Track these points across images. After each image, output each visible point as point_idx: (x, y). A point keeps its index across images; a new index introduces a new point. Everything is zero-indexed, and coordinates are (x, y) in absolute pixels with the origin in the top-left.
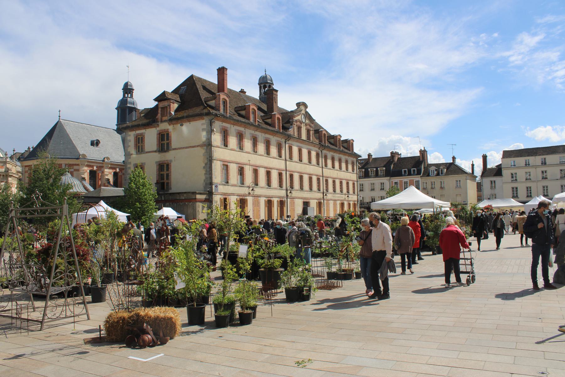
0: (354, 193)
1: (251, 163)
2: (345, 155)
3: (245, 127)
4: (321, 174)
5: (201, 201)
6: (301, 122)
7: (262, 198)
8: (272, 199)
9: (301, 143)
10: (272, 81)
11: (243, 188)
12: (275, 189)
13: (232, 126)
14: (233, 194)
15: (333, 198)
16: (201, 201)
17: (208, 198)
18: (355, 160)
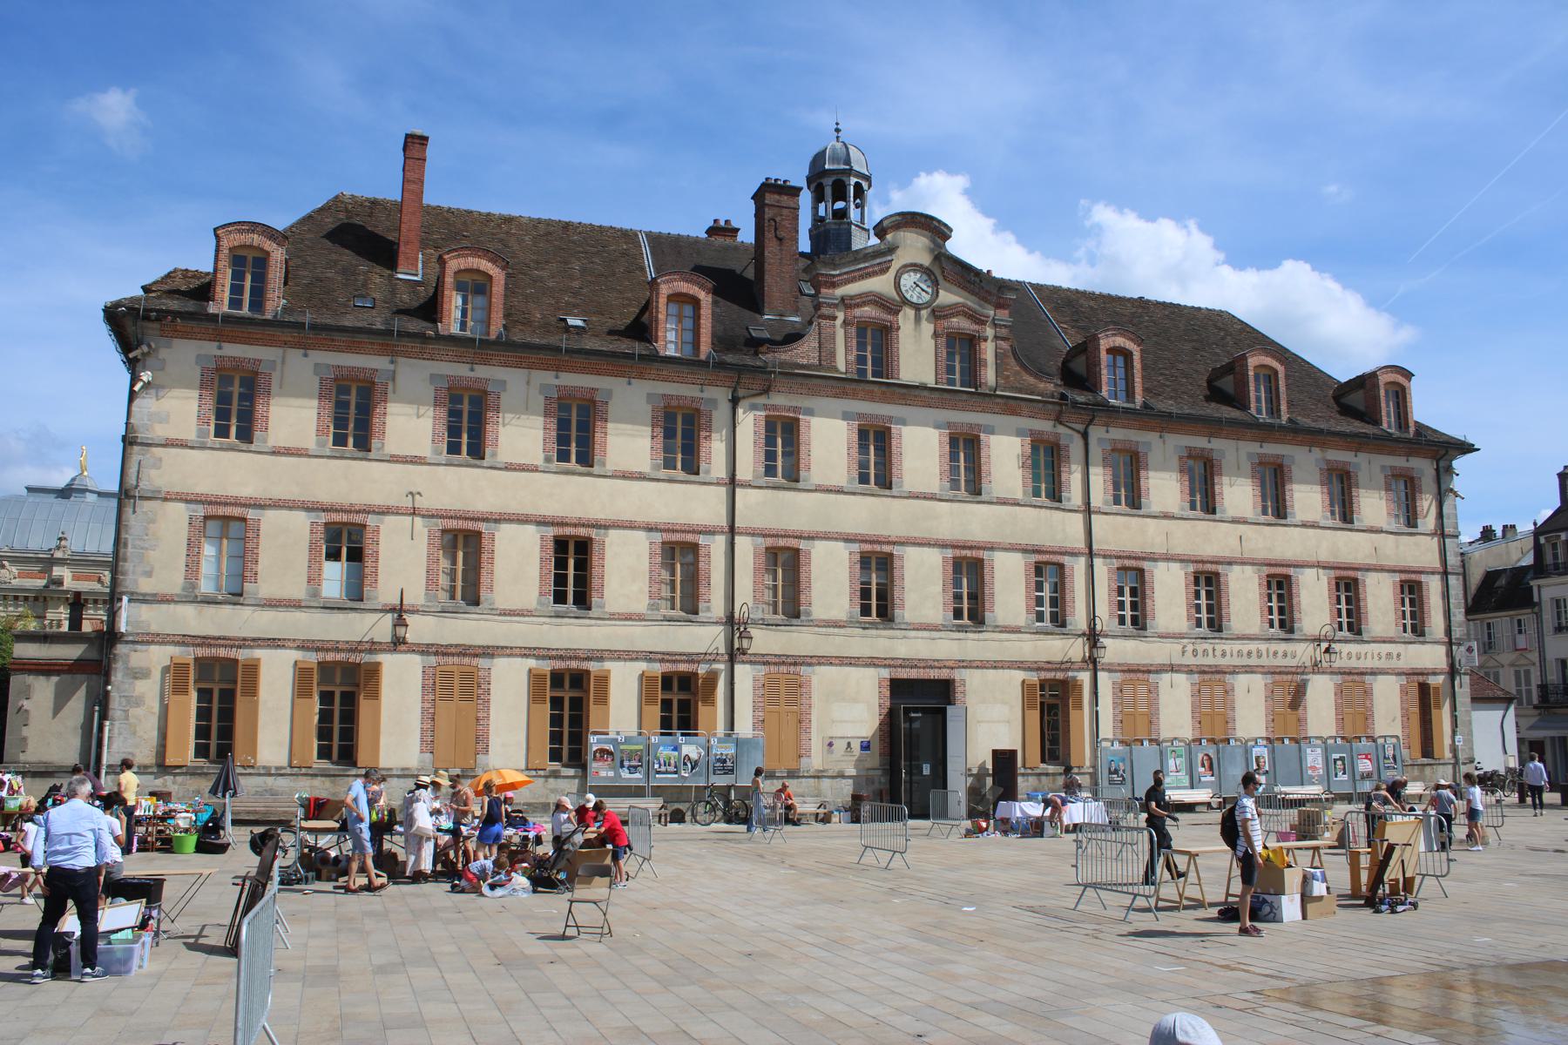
0: (1418, 630)
1: (421, 503)
2: (1323, 446)
3: (392, 352)
4: (1081, 544)
5: (44, 669)
6: (892, 306)
7: (500, 665)
8: (593, 666)
9: (885, 399)
10: (848, 161)
11: (352, 615)
12: (629, 617)
13: (294, 355)
14: (274, 643)
15: (1189, 660)
16: (44, 669)
17: (94, 655)
18: (1424, 467)
